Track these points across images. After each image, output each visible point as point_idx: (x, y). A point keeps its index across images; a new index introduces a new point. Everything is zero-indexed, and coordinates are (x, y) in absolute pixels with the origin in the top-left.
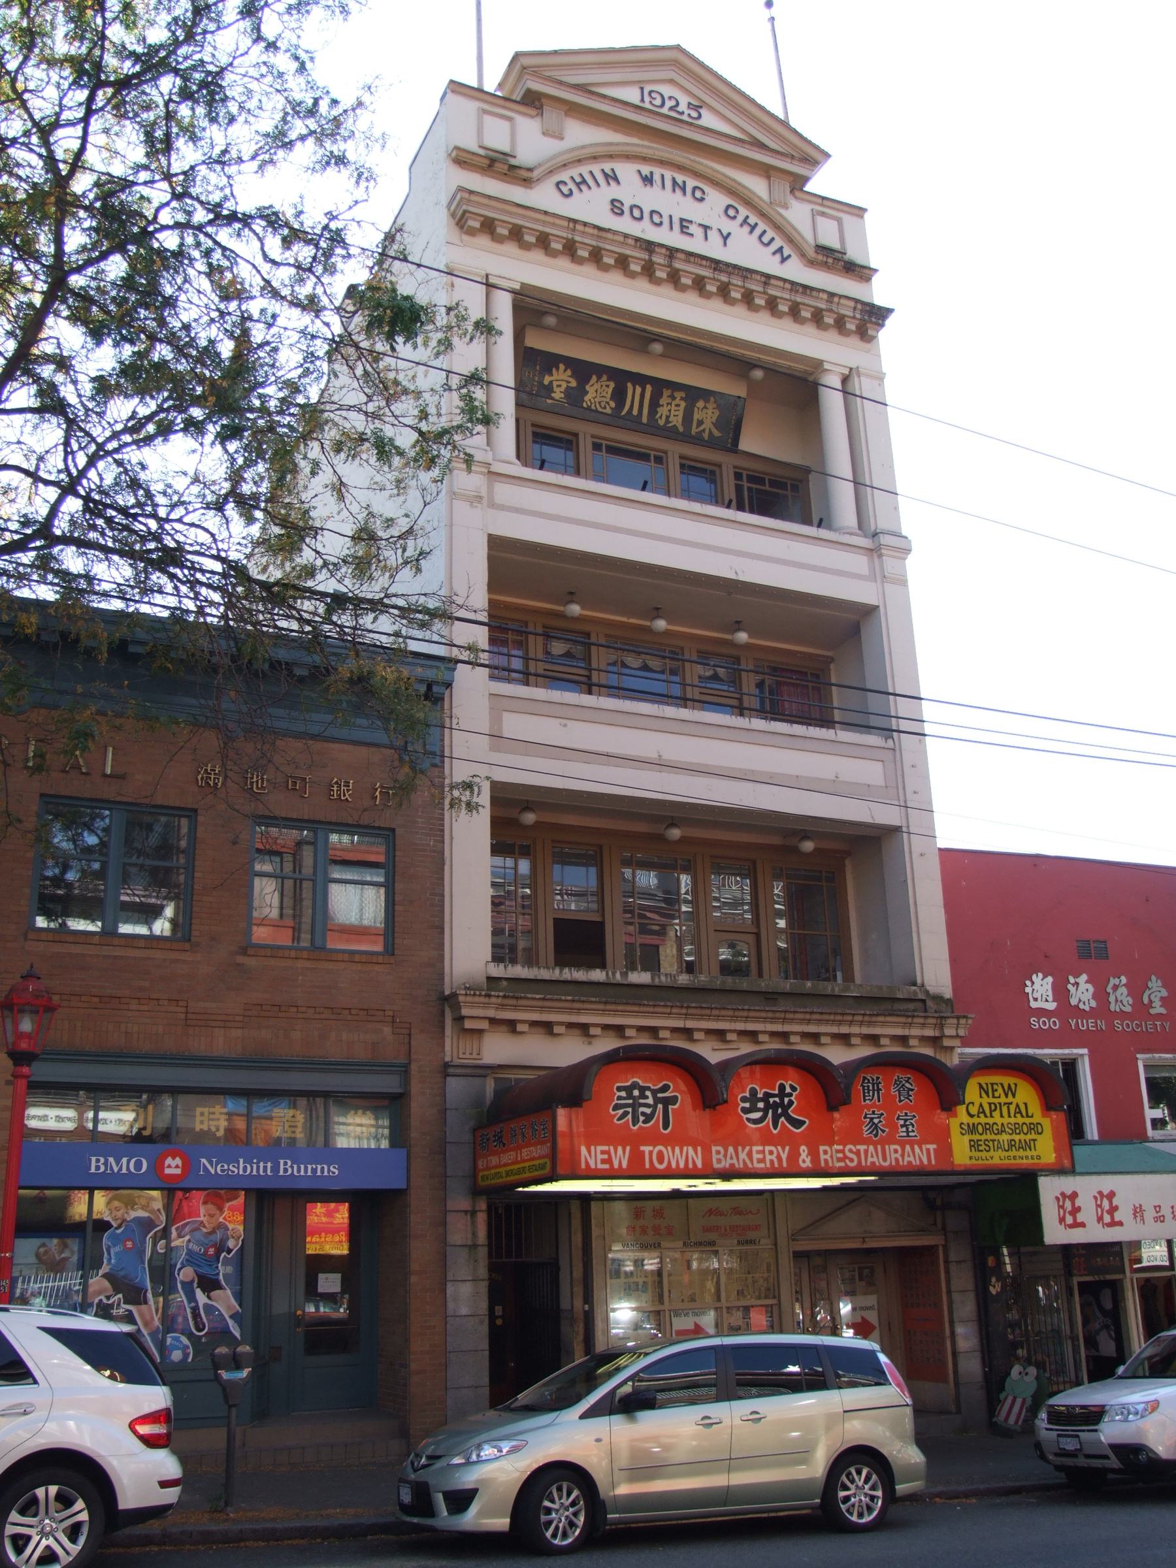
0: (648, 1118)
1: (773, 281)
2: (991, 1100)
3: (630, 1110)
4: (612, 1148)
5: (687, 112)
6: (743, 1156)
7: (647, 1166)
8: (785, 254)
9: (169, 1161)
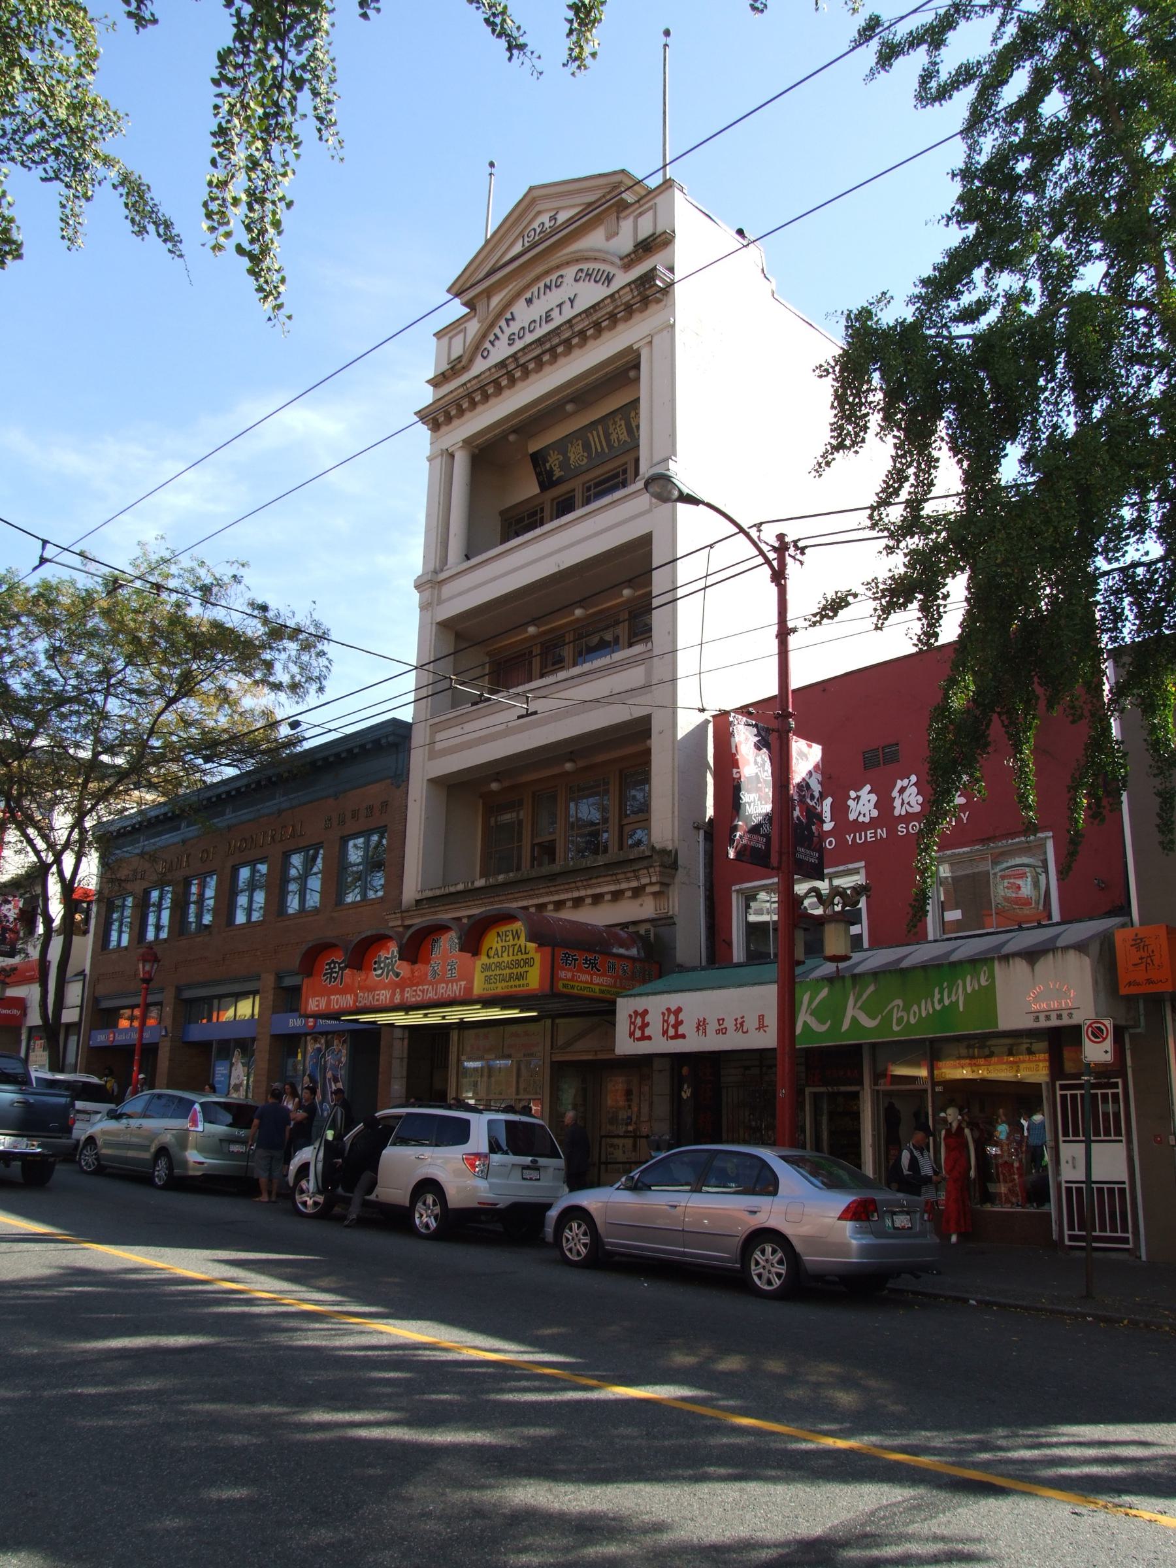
2: (504, 944)
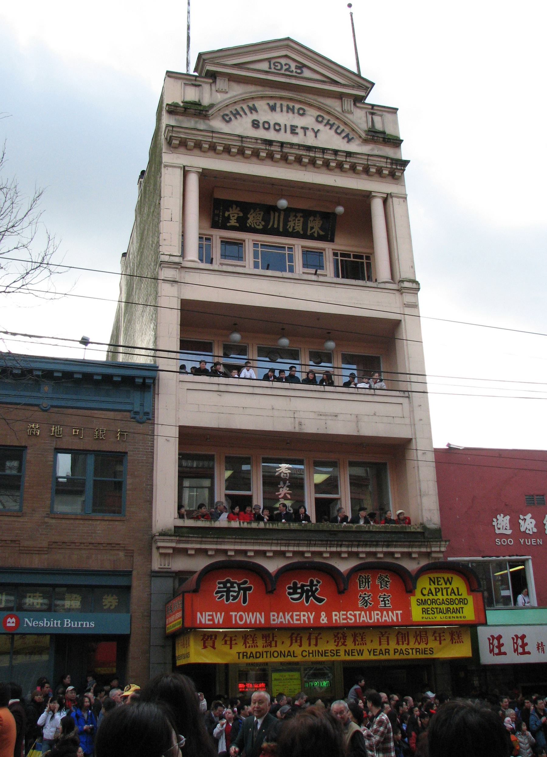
0: (235, 598)
1: (339, 153)
2: (436, 586)
3: (225, 594)
4: (214, 613)
5: (294, 71)
6: (288, 617)
7: (234, 622)
8: (350, 137)
9: (9, 620)
